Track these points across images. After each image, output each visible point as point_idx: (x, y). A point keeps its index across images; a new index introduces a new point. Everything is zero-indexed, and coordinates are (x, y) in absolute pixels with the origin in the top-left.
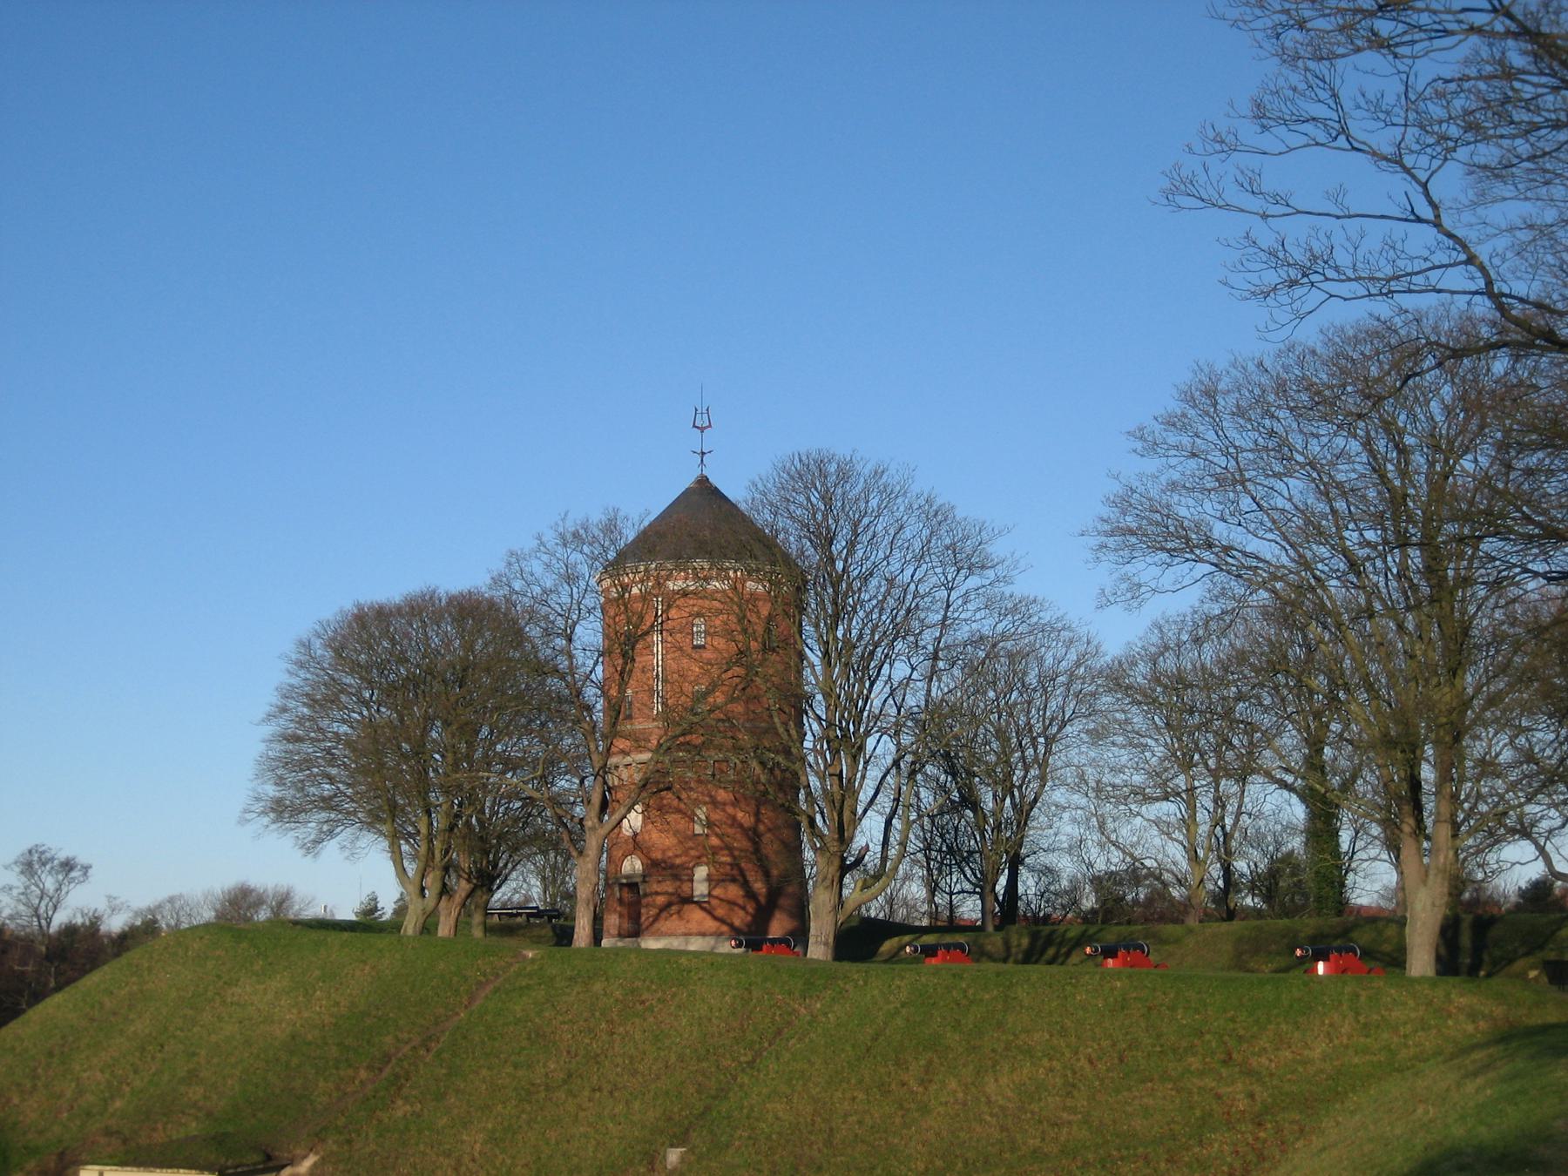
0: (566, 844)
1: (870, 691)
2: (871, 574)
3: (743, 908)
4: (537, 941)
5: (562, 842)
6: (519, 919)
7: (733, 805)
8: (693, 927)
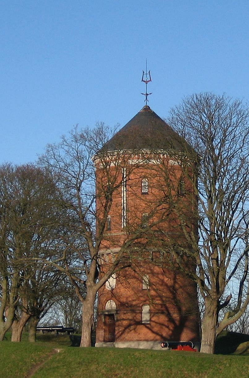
0: (77, 294)
1: (232, 216)
2: (233, 156)
3: (168, 327)
4: (62, 344)
5: (74, 293)
6: (53, 333)
7: (162, 274)
8: (142, 336)
